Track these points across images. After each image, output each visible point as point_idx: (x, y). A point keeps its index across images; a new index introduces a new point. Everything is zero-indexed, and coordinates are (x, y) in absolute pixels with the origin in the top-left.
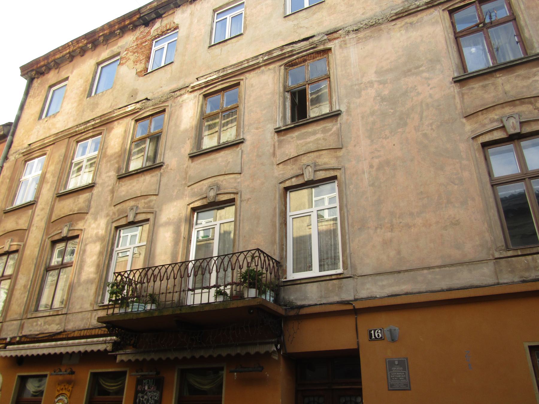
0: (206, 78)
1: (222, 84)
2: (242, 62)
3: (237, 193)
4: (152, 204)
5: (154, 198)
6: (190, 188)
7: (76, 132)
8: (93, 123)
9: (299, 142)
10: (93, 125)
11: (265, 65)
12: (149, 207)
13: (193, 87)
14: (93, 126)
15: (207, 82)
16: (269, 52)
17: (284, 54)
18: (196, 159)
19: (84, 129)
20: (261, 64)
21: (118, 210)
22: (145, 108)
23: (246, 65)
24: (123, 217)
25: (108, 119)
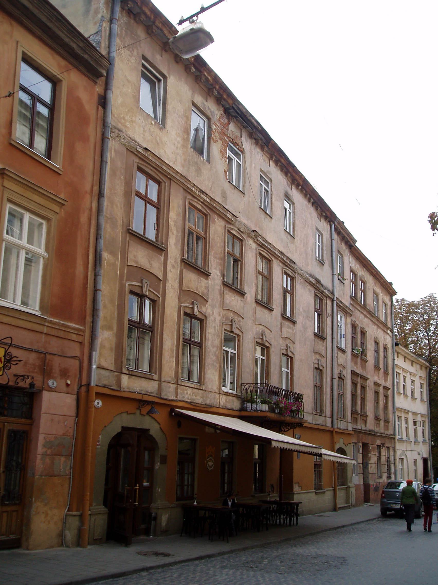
0: (263, 241)
1: (266, 253)
2: (276, 249)
3: (271, 345)
4: (241, 323)
5: (241, 319)
6: (255, 326)
7: (192, 191)
8: (205, 198)
9: (288, 330)
10: (204, 200)
11: (280, 260)
12: (239, 325)
13: (258, 240)
14: (204, 200)
15: (263, 245)
16: (284, 255)
17: (286, 262)
18: (257, 305)
19: (198, 196)
20: (280, 259)
21: (225, 314)
22: (233, 225)
23: (276, 253)
24: (229, 324)
25: (215, 207)
